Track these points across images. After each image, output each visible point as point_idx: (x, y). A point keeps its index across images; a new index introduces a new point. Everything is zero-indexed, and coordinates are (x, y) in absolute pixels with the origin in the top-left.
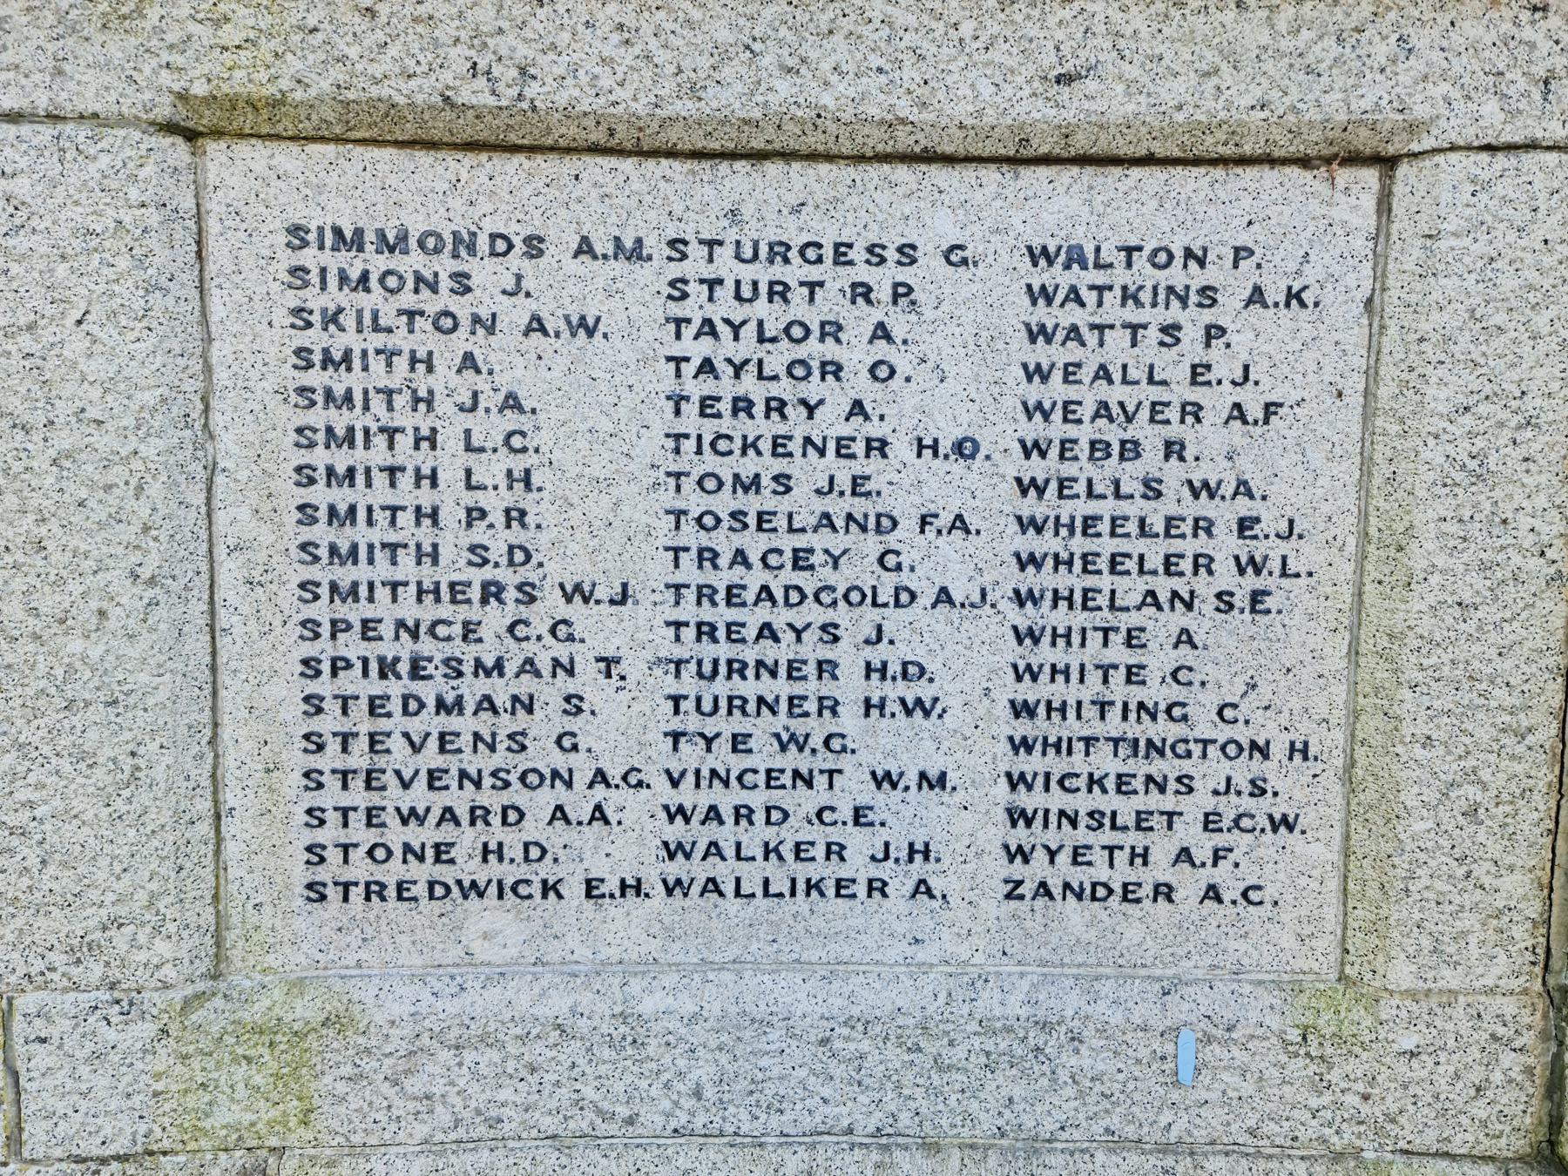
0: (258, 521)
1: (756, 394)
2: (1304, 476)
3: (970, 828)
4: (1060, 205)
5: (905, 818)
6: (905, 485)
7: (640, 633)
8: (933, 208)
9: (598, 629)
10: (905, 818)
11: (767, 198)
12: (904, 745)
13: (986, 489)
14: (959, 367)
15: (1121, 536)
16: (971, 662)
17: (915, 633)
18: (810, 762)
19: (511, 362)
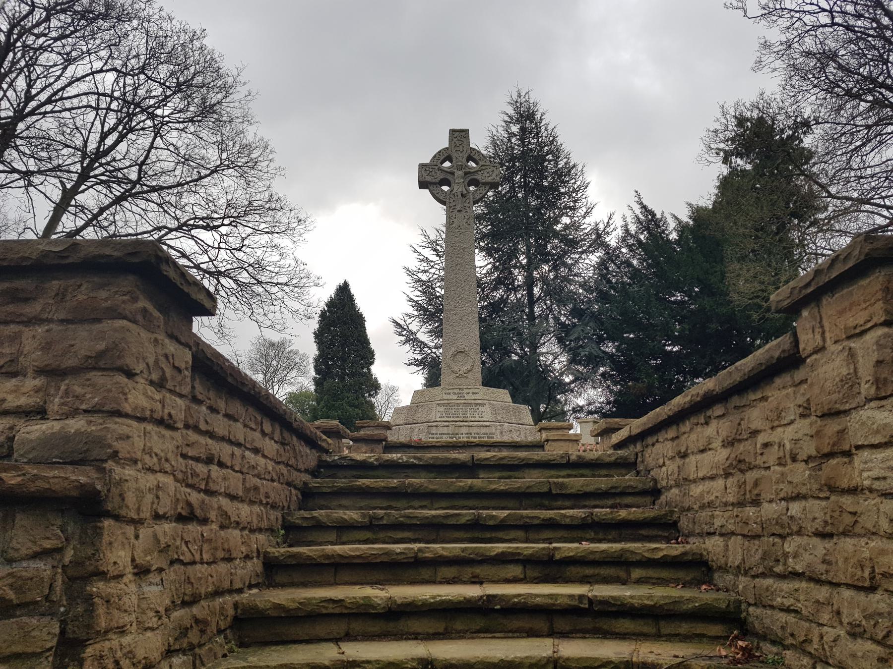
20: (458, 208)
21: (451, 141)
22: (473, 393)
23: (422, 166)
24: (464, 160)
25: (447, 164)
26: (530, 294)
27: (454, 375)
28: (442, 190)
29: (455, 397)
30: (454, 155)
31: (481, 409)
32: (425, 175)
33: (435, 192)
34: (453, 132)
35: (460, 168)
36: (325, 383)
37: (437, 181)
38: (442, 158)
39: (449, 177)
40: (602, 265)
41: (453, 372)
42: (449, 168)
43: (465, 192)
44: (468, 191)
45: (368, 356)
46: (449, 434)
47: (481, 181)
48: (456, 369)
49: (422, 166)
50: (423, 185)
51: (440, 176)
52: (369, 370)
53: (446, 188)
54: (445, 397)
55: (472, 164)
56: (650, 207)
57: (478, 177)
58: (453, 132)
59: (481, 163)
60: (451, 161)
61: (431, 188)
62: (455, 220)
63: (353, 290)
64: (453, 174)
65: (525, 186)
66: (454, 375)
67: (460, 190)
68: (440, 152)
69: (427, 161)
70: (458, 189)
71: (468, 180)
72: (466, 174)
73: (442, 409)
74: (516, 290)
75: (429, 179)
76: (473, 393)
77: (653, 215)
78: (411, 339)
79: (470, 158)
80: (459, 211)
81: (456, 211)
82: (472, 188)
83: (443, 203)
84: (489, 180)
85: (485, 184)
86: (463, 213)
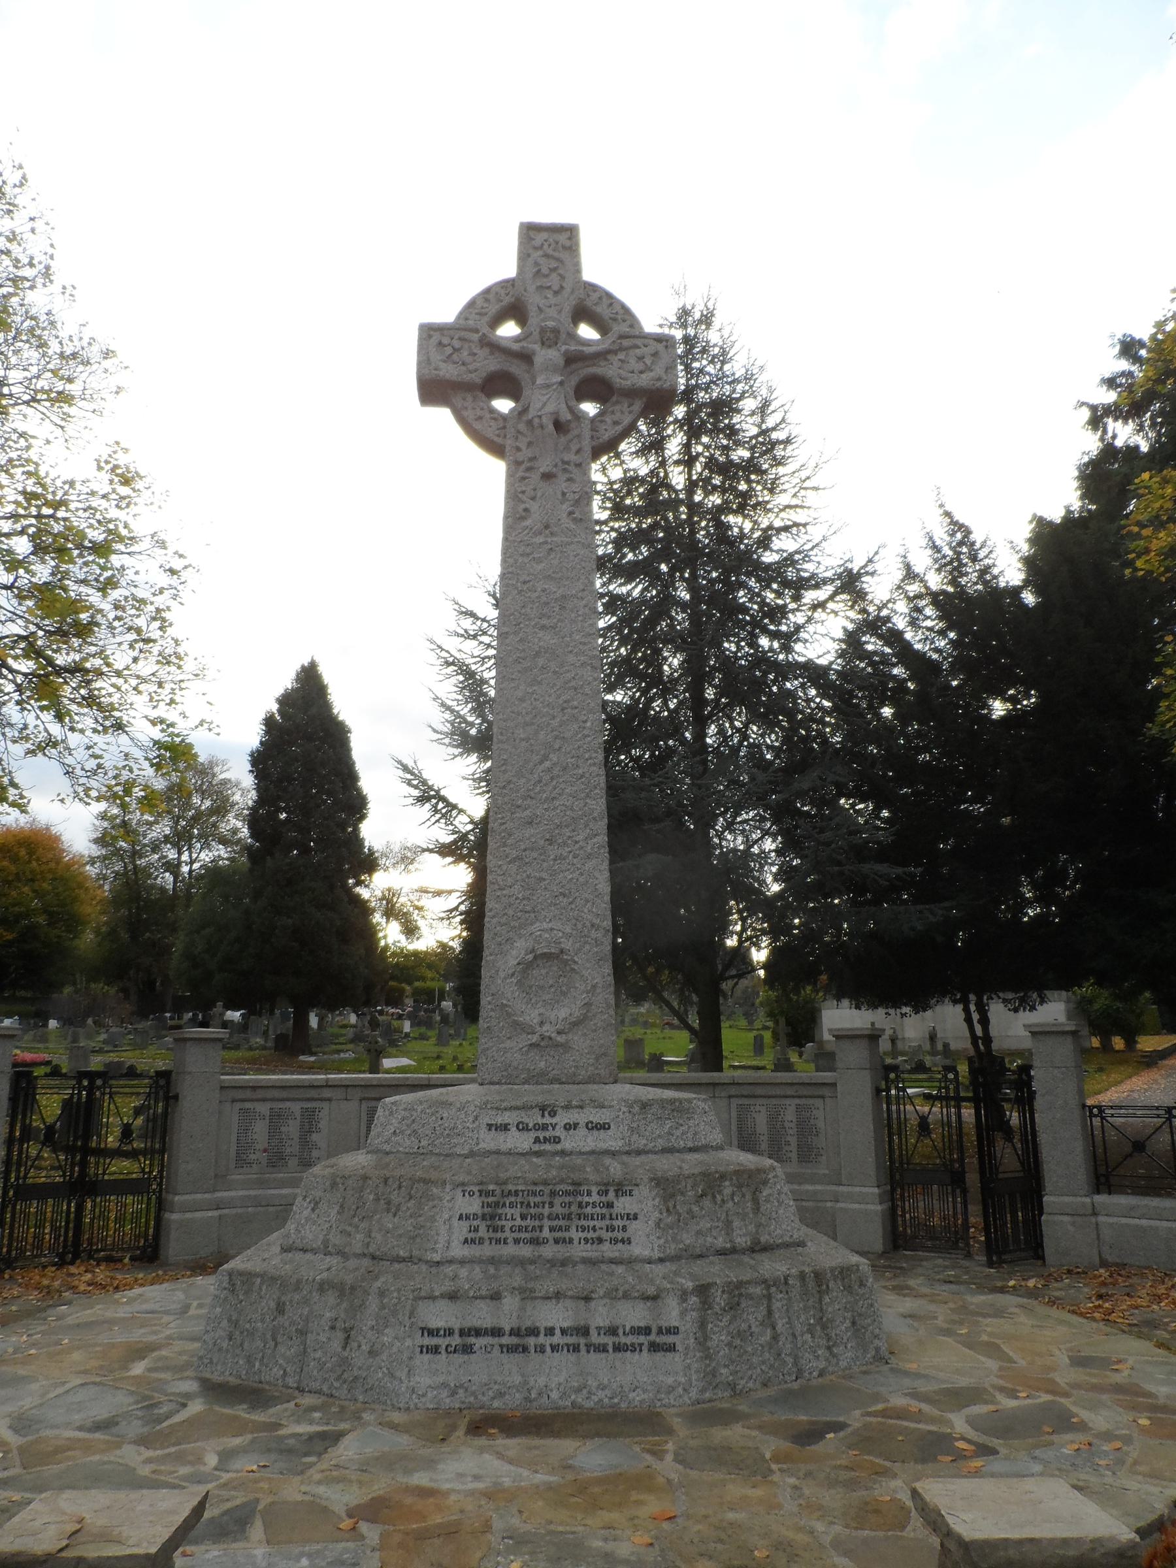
0: (734, 1128)
1: (774, 1119)
2: (821, 1124)
3: (794, 1155)
4: (797, 1101)
5: (789, 1155)
6: (787, 1124)
7: (765, 1138)
8: (788, 1101)
9: (762, 1138)
10: (789, 1155)
11: (774, 1101)
12: (786, 1148)
13: (793, 1125)
14: (790, 1115)
15: (805, 1129)
16: (793, 1141)
17: (789, 1138)
18: (780, 1149)
19: (754, 1115)
20: (545, 466)
21: (523, 257)
22: (593, 1127)
23: (430, 334)
24: (566, 317)
25: (509, 330)
26: (698, 701)
27: (525, 1040)
28: (493, 411)
29: (524, 1142)
30: (534, 300)
31: (624, 1205)
32: (436, 357)
33: (469, 414)
34: (531, 233)
35: (550, 337)
36: (269, 862)
37: (477, 378)
38: (494, 309)
39: (517, 369)
40: (852, 641)
41: (521, 1028)
42: (517, 339)
43: (566, 416)
44: (579, 416)
45: (356, 806)
46: (496, 1332)
47: (618, 382)
48: (531, 1016)
49: (430, 334)
50: (433, 390)
51: (490, 364)
52: (356, 830)
53: (503, 405)
54: (490, 1140)
55: (586, 332)
56: (959, 517)
57: (610, 370)
58: (531, 233)
59: (619, 328)
60: (522, 321)
61: (458, 401)
62: (534, 506)
63: (328, 675)
64: (526, 358)
65: (688, 461)
66: (525, 1040)
67: (550, 408)
68: (488, 291)
69: (447, 313)
70: (546, 401)
71: (574, 381)
72: (571, 360)
73: (474, 1206)
74: (667, 690)
75: (450, 371)
76: (593, 1127)
77: (968, 532)
78: (428, 795)
79: (582, 313)
80: (547, 476)
81: (535, 477)
82: (590, 408)
83: (494, 448)
84: (644, 381)
85: (632, 393)
86: (561, 484)
